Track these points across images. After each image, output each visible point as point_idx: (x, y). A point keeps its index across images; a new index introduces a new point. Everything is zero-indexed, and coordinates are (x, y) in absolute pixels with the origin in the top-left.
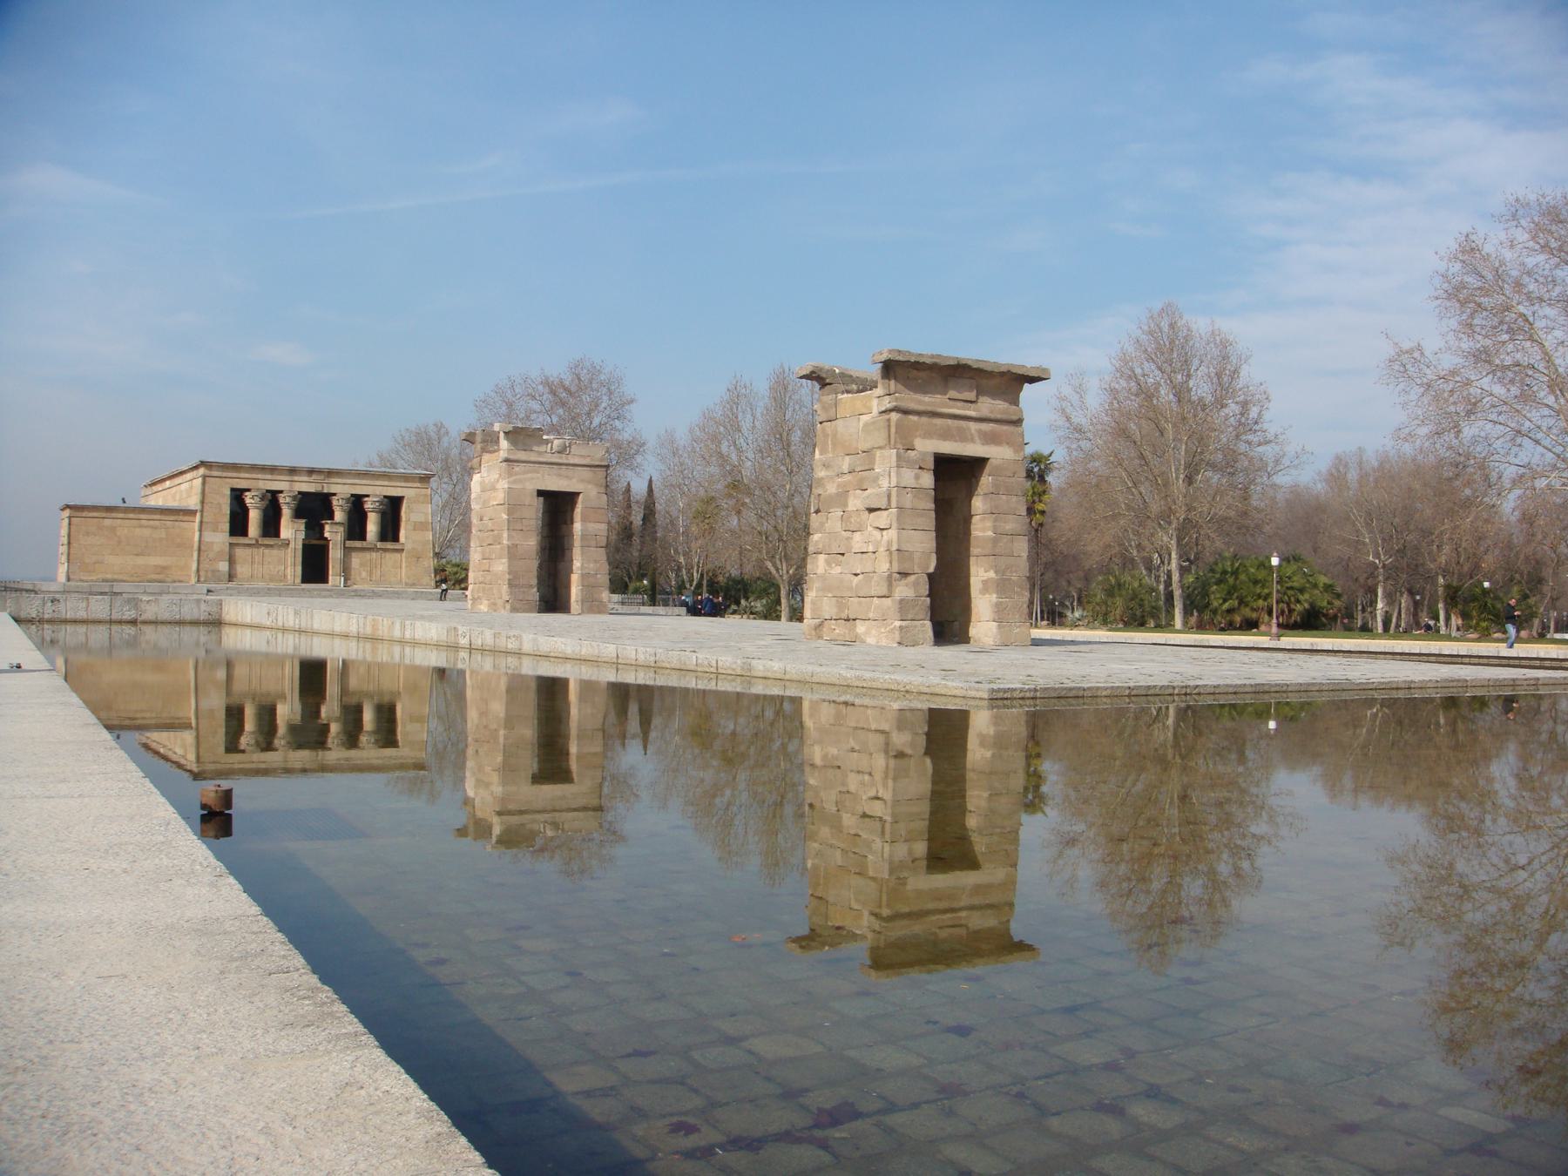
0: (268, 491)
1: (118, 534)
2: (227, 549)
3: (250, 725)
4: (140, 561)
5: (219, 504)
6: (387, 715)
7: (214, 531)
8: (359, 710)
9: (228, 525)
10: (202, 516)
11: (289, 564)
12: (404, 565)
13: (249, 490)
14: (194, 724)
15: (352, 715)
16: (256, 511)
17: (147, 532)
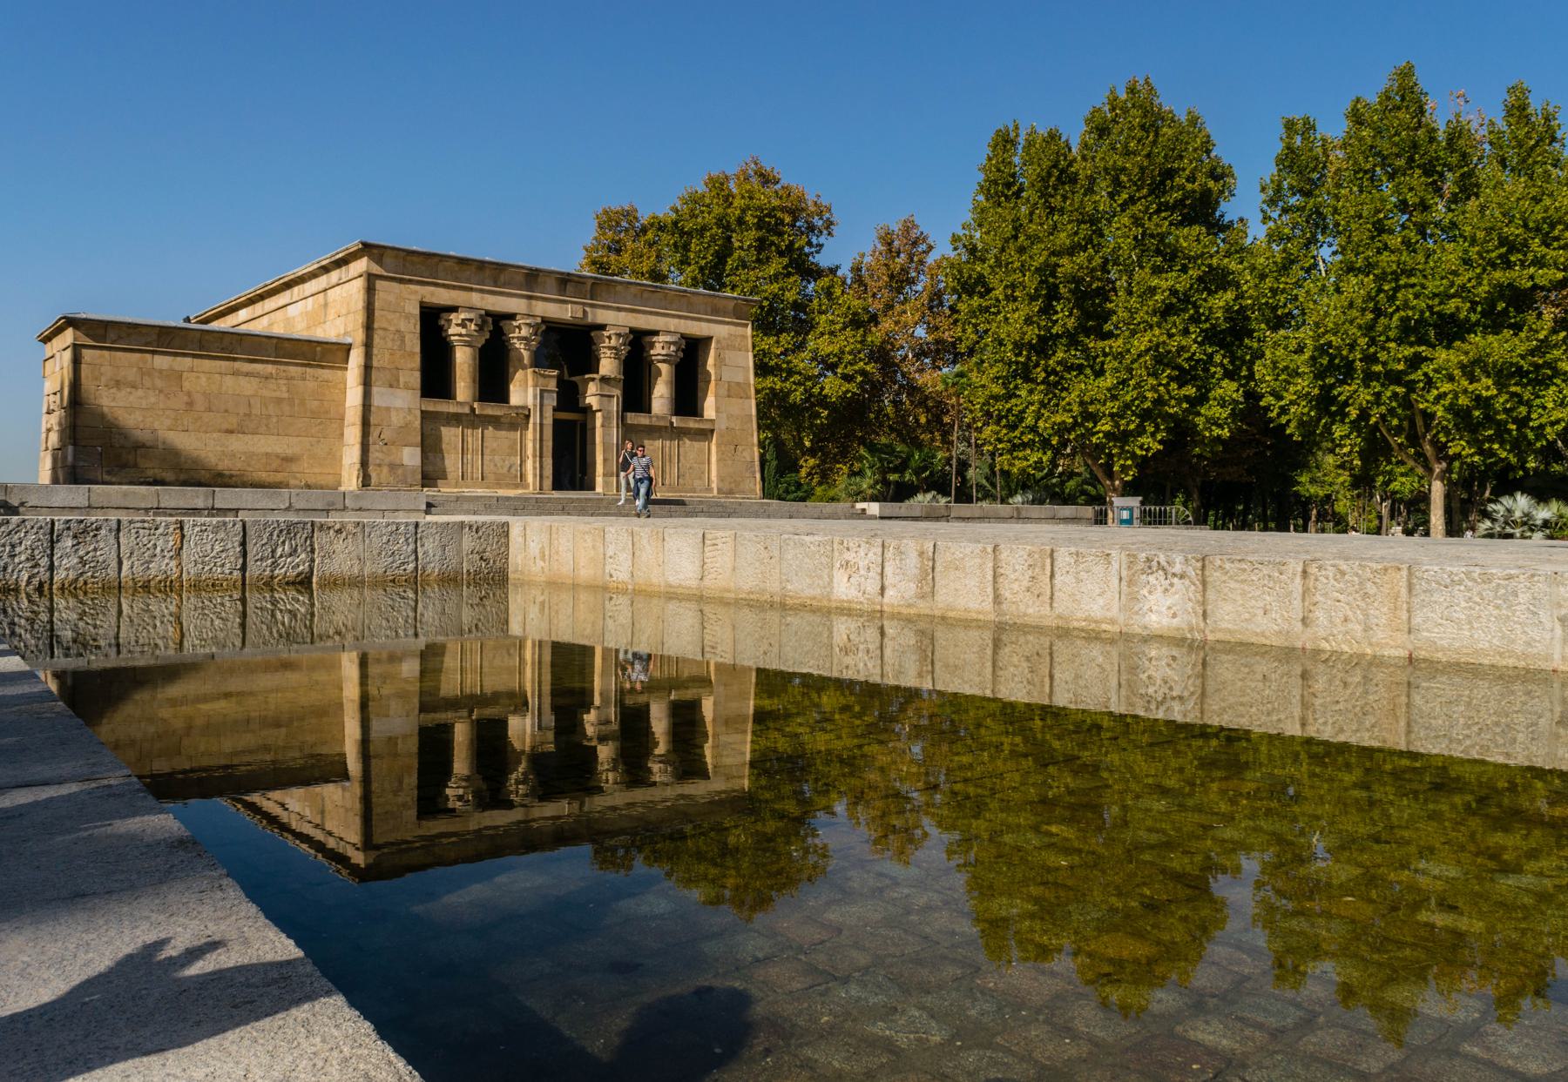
0: (488, 313)
1: (186, 385)
2: (417, 423)
3: (461, 765)
4: (237, 444)
5: (398, 331)
6: (686, 719)
7: (391, 386)
8: (641, 715)
9: (418, 374)
10: (368, 355)
11: (530, 452)
12: (714, 459)
13: (454, 309)
14: (354, 765)
15: (633, 723)
16: (468, 350)
17: (248, 386)
